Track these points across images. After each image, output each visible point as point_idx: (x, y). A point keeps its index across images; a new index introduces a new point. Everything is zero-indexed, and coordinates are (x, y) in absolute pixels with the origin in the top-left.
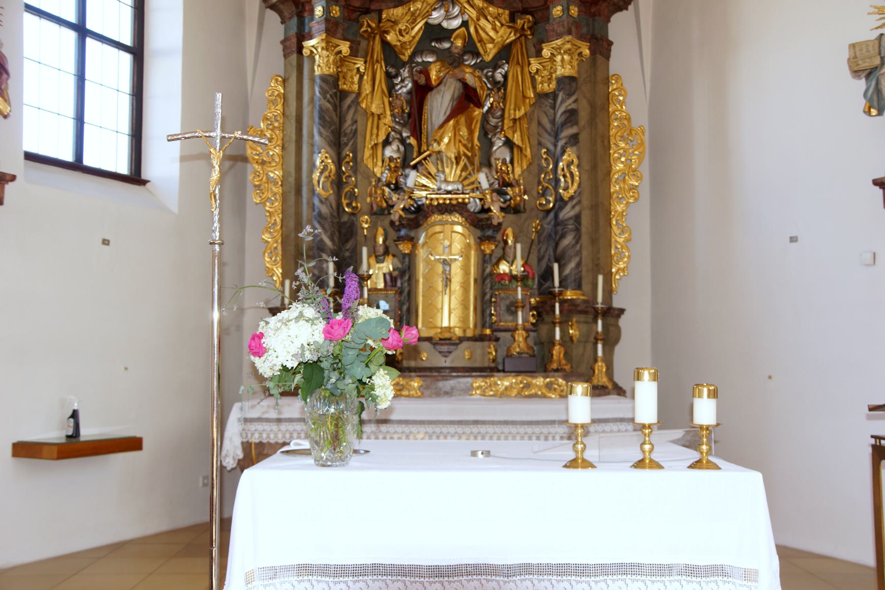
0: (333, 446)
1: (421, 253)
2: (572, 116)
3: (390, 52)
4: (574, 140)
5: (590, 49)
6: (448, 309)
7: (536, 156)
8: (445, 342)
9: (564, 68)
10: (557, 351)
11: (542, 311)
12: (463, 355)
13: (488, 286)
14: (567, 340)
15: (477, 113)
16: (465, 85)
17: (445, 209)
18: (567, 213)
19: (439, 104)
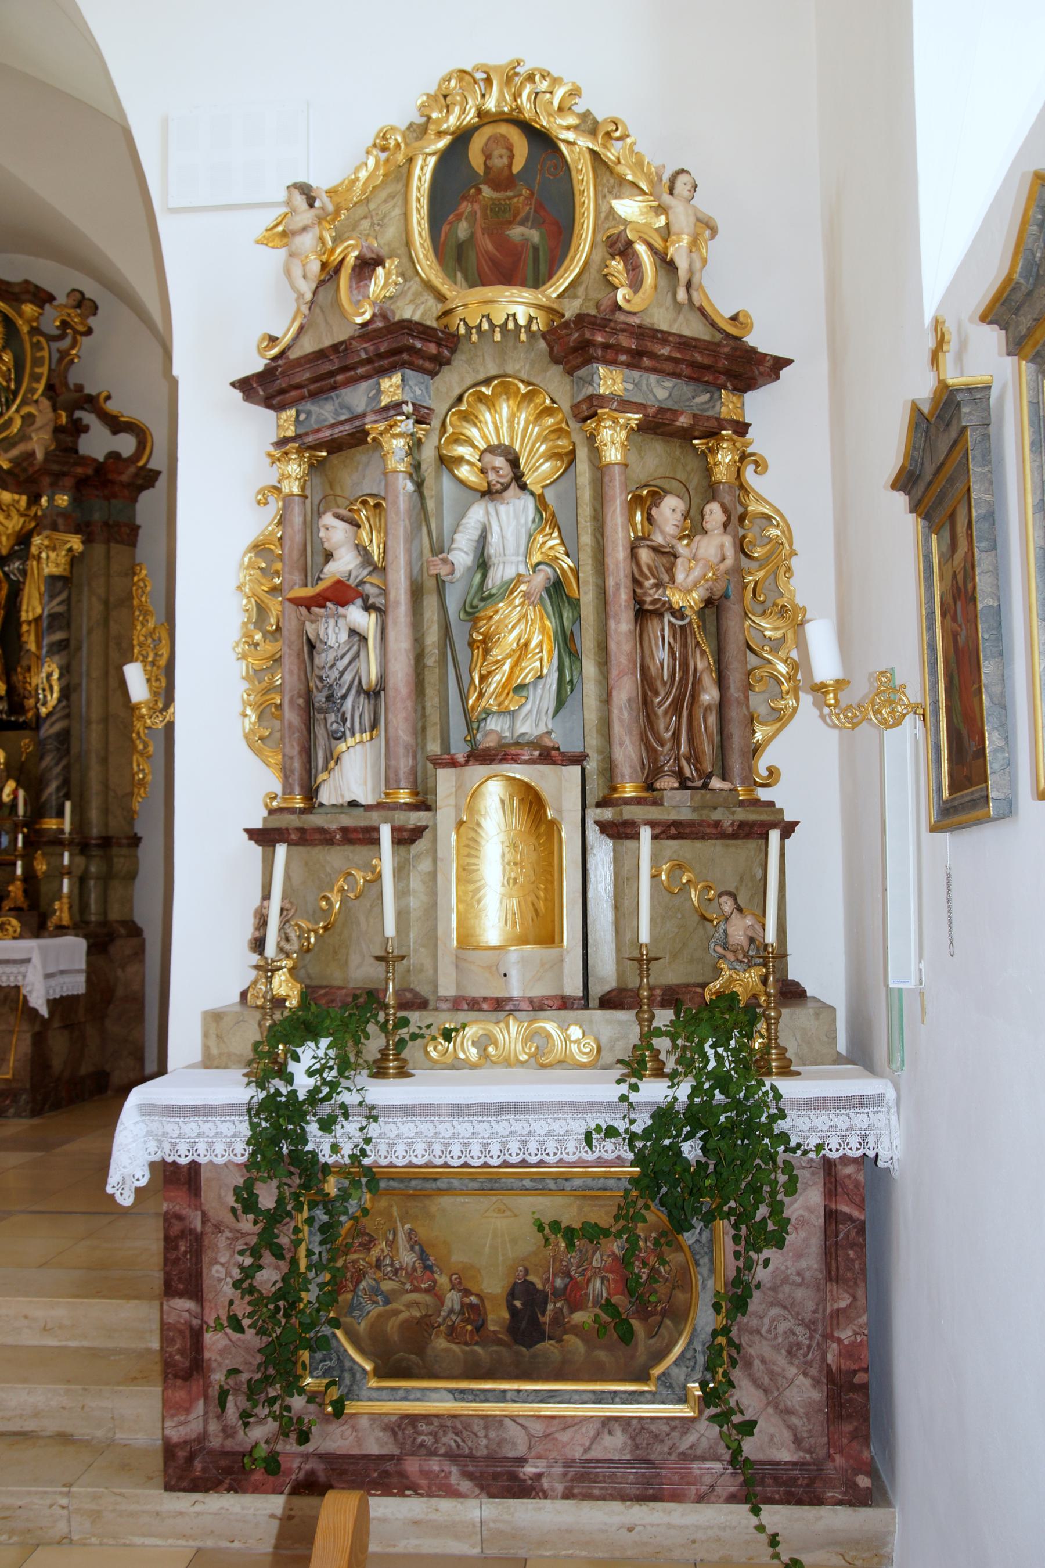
5: (83, 542)
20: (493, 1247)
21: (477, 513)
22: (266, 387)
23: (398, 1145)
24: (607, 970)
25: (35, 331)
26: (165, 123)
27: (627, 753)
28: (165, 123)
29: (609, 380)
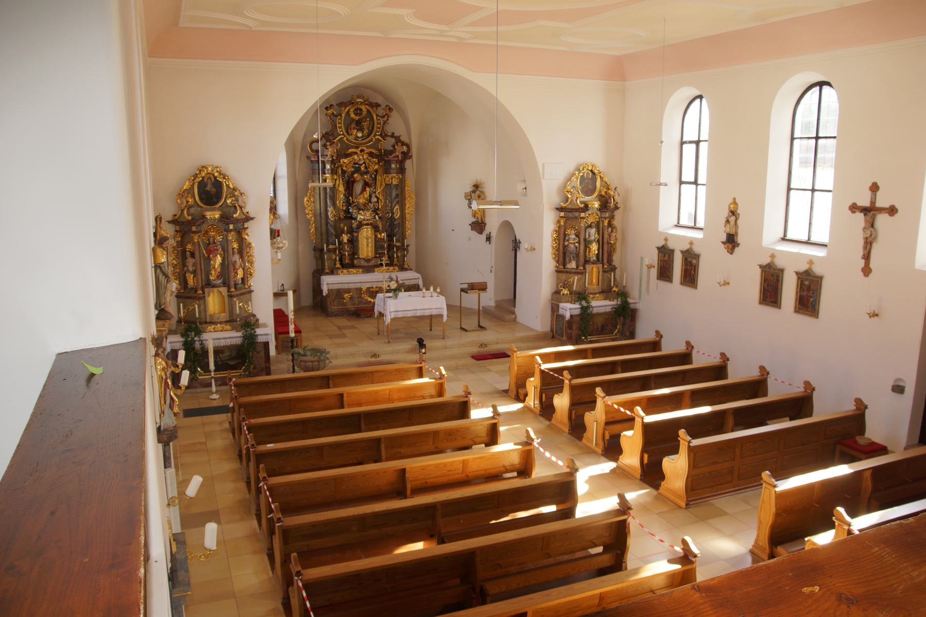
1: (360, 237)
2: (397, 196)
3: (344, 172)
4: (398, 202)
6: (366, 248)
7: (385, 202)
8: (368, 260)
10: (395, 260)
11: (390, 247)
12: (373, 263)
13: (378, 244)
14: (397, 256)
15: (368, 189)
18: (396, 222)
19: (358, 187)
20: (599, 321)
21: (588, 230)
22: (560, 209)
23: (595, 311)
25: (377, 116)
26: (543, 165)
28: (543, 165)
29: (607, 215)
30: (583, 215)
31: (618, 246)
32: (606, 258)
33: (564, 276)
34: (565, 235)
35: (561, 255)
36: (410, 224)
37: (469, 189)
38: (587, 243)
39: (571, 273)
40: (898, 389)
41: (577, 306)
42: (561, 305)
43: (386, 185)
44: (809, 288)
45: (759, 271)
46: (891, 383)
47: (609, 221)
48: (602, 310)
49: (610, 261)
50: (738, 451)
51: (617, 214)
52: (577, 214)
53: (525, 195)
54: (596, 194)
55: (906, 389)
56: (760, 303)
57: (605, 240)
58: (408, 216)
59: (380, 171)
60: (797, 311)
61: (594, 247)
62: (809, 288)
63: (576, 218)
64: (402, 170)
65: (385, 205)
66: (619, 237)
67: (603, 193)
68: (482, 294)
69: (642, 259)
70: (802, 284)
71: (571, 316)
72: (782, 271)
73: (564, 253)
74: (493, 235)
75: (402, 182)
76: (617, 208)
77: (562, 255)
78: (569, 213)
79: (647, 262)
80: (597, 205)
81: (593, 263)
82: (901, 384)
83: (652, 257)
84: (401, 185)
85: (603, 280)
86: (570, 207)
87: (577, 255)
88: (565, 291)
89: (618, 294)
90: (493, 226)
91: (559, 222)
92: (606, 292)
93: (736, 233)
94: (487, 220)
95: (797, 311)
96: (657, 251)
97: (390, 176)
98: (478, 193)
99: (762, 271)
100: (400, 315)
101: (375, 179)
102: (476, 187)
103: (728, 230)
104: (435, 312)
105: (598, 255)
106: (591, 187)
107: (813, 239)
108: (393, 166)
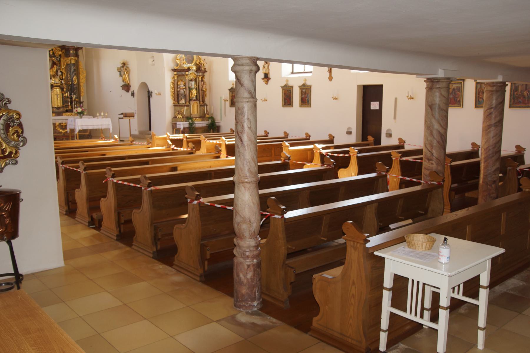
0: (81, 117)
2: (75, 70)
4: (75, 74)
7: (67, 75)
9: (73, 62)
12: (61, 110)
15: (55, 66)
16: (53, 61)
17: (57, 86)
18: (75, 86)
21: (191, 82)
22: (174, 70)
23: (197, 126)
24: (202, 115)
27: (201, 100)
29: (200, 74)
30: (187, 73)
31: (207, 93)
32: (201, 98)
33: (178, 108)
34: (178, 85)
35: (176, 96)
36: (83, 89)
37: (120, 65)
38: (190, 89)
39: (182, 106)
40: (349, 133)
41: (188, 123)
42: (178, 123)
43: (67, 64)
44: (305, 93)
45: (281, 90)
46: (346, 131)
47: (202, 78)
48: (201, 125)
49: (203, 101)
50: (273, 151)
51: (206, 74)
52: (183, 73)
53: (154, 65)
54: (193, 63)
55: (353, 133)
56: (283, 106)
57: (200, 88)
58: (82, 84)
59: (63, 56)
60: (301, 106)
61: (194, 92)
62: (305, 93)
63: (183, 75)
64: (77, 55)
65: (67, 77)
66: (208, 88)
67: (198, 63)
68: (131, 118)
69: (221, 98)
70: (302, 92)
71: (184, 128)
72: (292, 87)
73: (178, 95)
74: (136, 92)
75: (77, 62)
76: (205, 71)
77: (177, 96)
78: (179, 72)
79: (223, 98)
80: (194, 68)
81: (194, 100)
82: (351, 131)
83: (227, 95)
84: (77, 64)
85: (200, 110)
86: (180, 68)
87: (185, 96)
88: (180, 116)
89: (209, 118)
90: (135, 87)
91: (174, 77)
92: (203, 117)
93: (269, 73)
94: (131, 84)
95: (301, 106)
96: (228, 91)
97: (69, 58)
98: (125, 67)
99: (283, 89)
100: (85, 128)
101: (60, 61)
102: (124, 64)
103: (264, 71)
104: (104, 127)
105: (196, 96)
106: (190, 59)
107: (306, 71)
108: (71, 52)
